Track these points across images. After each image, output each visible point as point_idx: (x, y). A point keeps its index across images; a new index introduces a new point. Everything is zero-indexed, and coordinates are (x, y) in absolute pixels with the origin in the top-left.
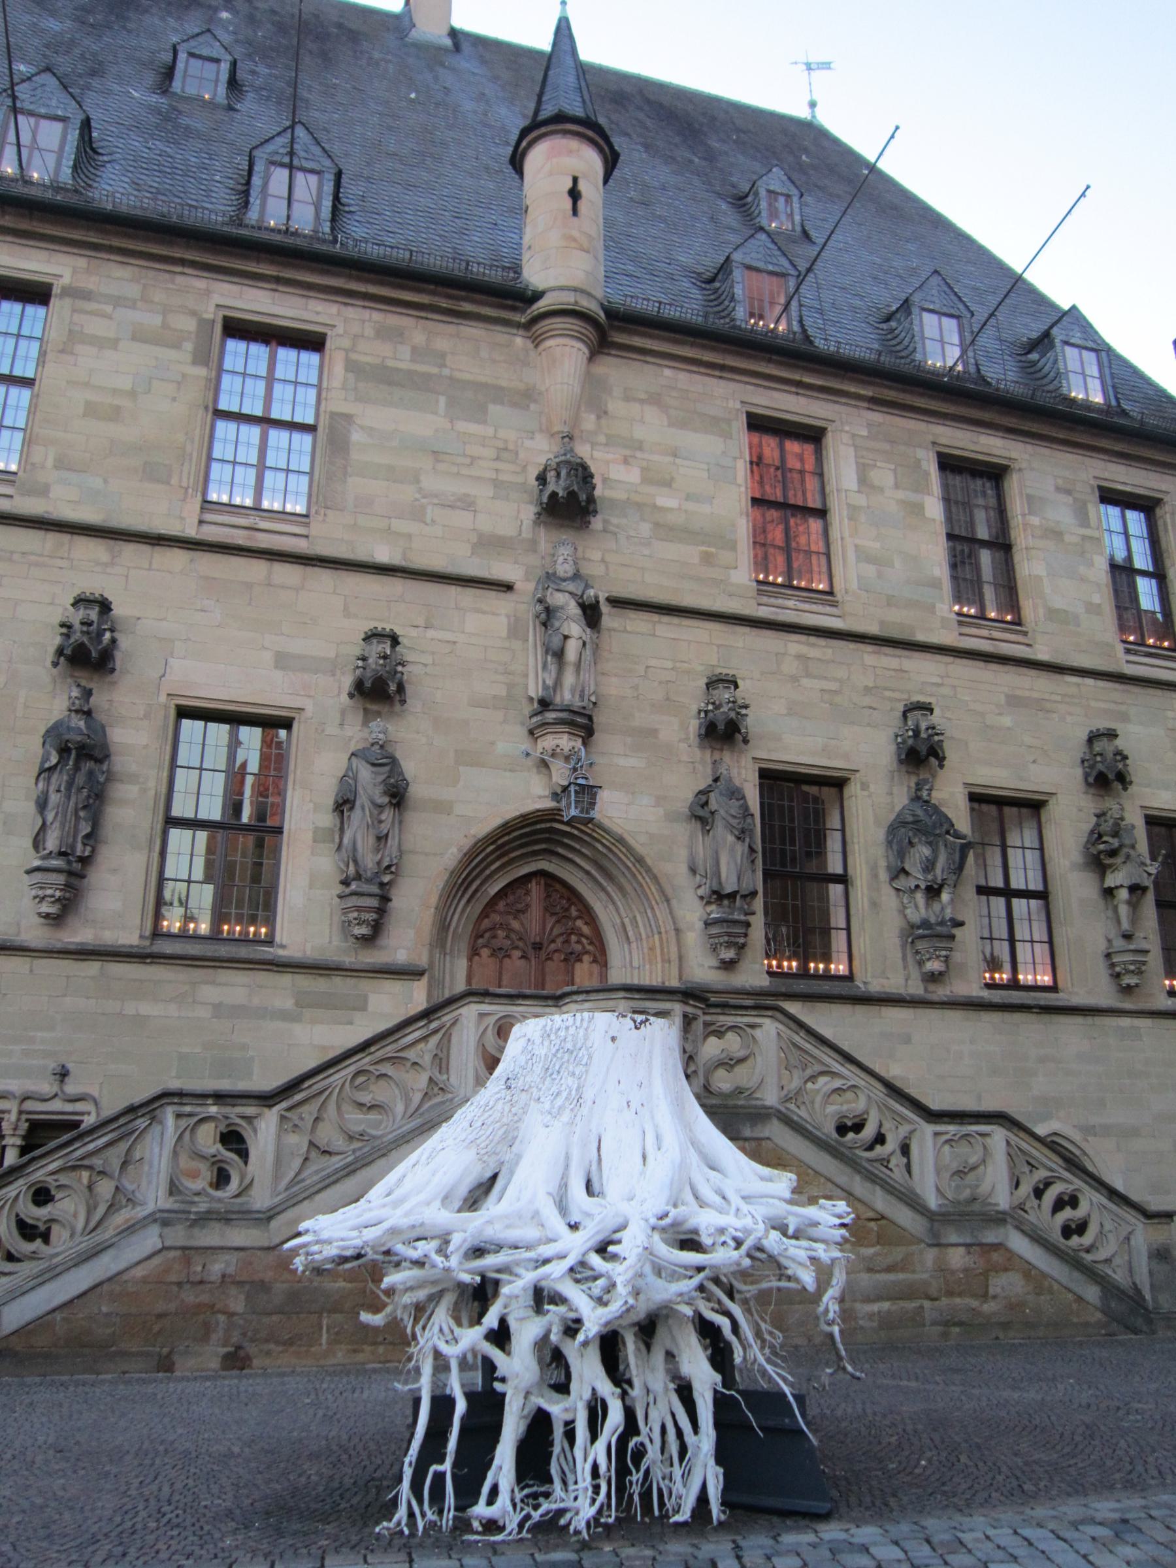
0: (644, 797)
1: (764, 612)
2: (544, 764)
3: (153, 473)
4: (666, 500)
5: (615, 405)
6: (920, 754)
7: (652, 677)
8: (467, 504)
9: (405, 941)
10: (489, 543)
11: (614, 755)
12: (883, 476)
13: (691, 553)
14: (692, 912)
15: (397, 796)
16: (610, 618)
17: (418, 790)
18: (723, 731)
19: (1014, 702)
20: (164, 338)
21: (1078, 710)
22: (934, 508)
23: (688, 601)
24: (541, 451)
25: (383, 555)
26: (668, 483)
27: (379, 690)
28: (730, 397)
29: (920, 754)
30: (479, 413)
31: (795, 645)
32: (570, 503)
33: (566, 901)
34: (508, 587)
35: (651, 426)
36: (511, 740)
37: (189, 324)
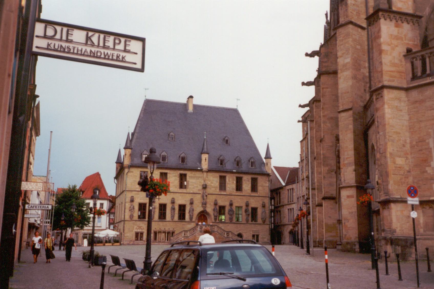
0: (210, 209)
1: (220, 193)
2: (203, 207)
3: (176, 187)
4: (212, 185)
5: (209, 177)
6: (231, 205)
7: (210, 200)
8: (197, 187)
9: (194, 220)
10: (199, 190)
11: (208, 205)
12: (231, 180)
13: (214, 189)
14: (213, 217)
15: (193, 210)
16: (208, 196)
17: (195, 209)
18: (216, 204)
19: (240, 199)
20: (175, 176)
21: (245, 200)
22: (235, 182)
23: (214, 193)
24: (203, 182)
25: (192, 192)
26: (212, 183)
27: (192, 203)
28: (218, 175)
29: (231, 205)
30: (198, 179)
31: (222, 196)
32: (205, 187)
33: (205, 216)
34: (200, 194)
35: (211, 178)
36: (201, 205)
37: (177, 175)
